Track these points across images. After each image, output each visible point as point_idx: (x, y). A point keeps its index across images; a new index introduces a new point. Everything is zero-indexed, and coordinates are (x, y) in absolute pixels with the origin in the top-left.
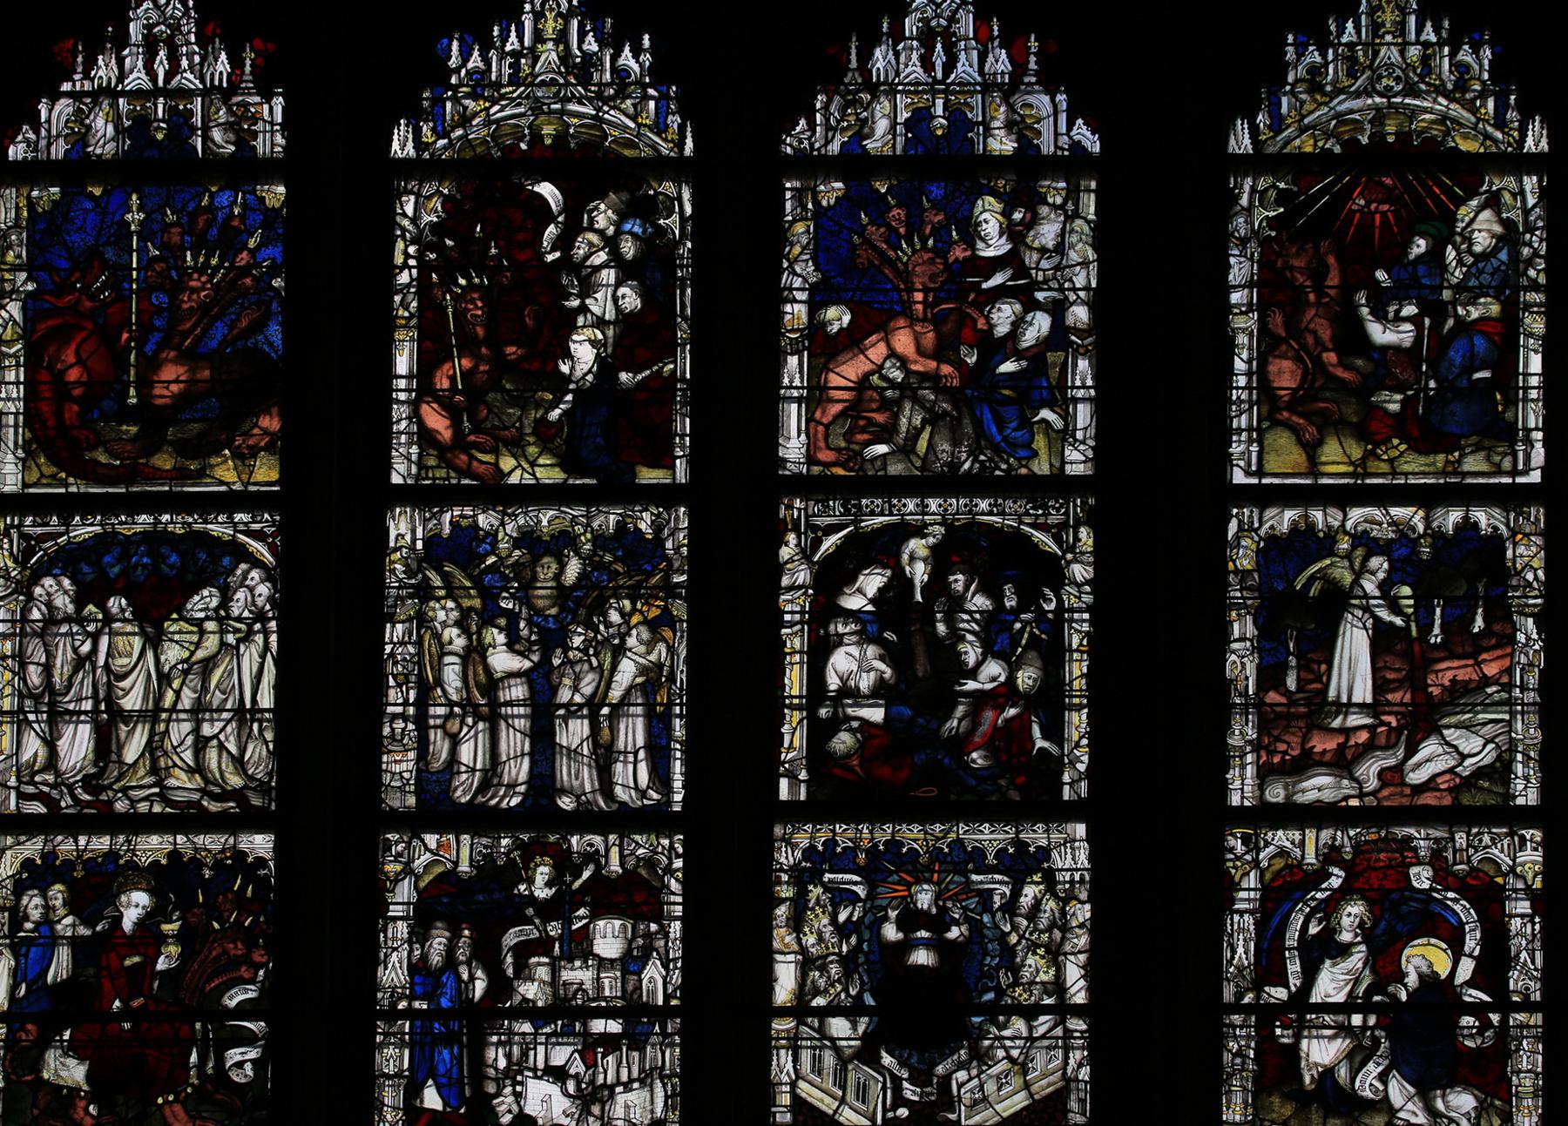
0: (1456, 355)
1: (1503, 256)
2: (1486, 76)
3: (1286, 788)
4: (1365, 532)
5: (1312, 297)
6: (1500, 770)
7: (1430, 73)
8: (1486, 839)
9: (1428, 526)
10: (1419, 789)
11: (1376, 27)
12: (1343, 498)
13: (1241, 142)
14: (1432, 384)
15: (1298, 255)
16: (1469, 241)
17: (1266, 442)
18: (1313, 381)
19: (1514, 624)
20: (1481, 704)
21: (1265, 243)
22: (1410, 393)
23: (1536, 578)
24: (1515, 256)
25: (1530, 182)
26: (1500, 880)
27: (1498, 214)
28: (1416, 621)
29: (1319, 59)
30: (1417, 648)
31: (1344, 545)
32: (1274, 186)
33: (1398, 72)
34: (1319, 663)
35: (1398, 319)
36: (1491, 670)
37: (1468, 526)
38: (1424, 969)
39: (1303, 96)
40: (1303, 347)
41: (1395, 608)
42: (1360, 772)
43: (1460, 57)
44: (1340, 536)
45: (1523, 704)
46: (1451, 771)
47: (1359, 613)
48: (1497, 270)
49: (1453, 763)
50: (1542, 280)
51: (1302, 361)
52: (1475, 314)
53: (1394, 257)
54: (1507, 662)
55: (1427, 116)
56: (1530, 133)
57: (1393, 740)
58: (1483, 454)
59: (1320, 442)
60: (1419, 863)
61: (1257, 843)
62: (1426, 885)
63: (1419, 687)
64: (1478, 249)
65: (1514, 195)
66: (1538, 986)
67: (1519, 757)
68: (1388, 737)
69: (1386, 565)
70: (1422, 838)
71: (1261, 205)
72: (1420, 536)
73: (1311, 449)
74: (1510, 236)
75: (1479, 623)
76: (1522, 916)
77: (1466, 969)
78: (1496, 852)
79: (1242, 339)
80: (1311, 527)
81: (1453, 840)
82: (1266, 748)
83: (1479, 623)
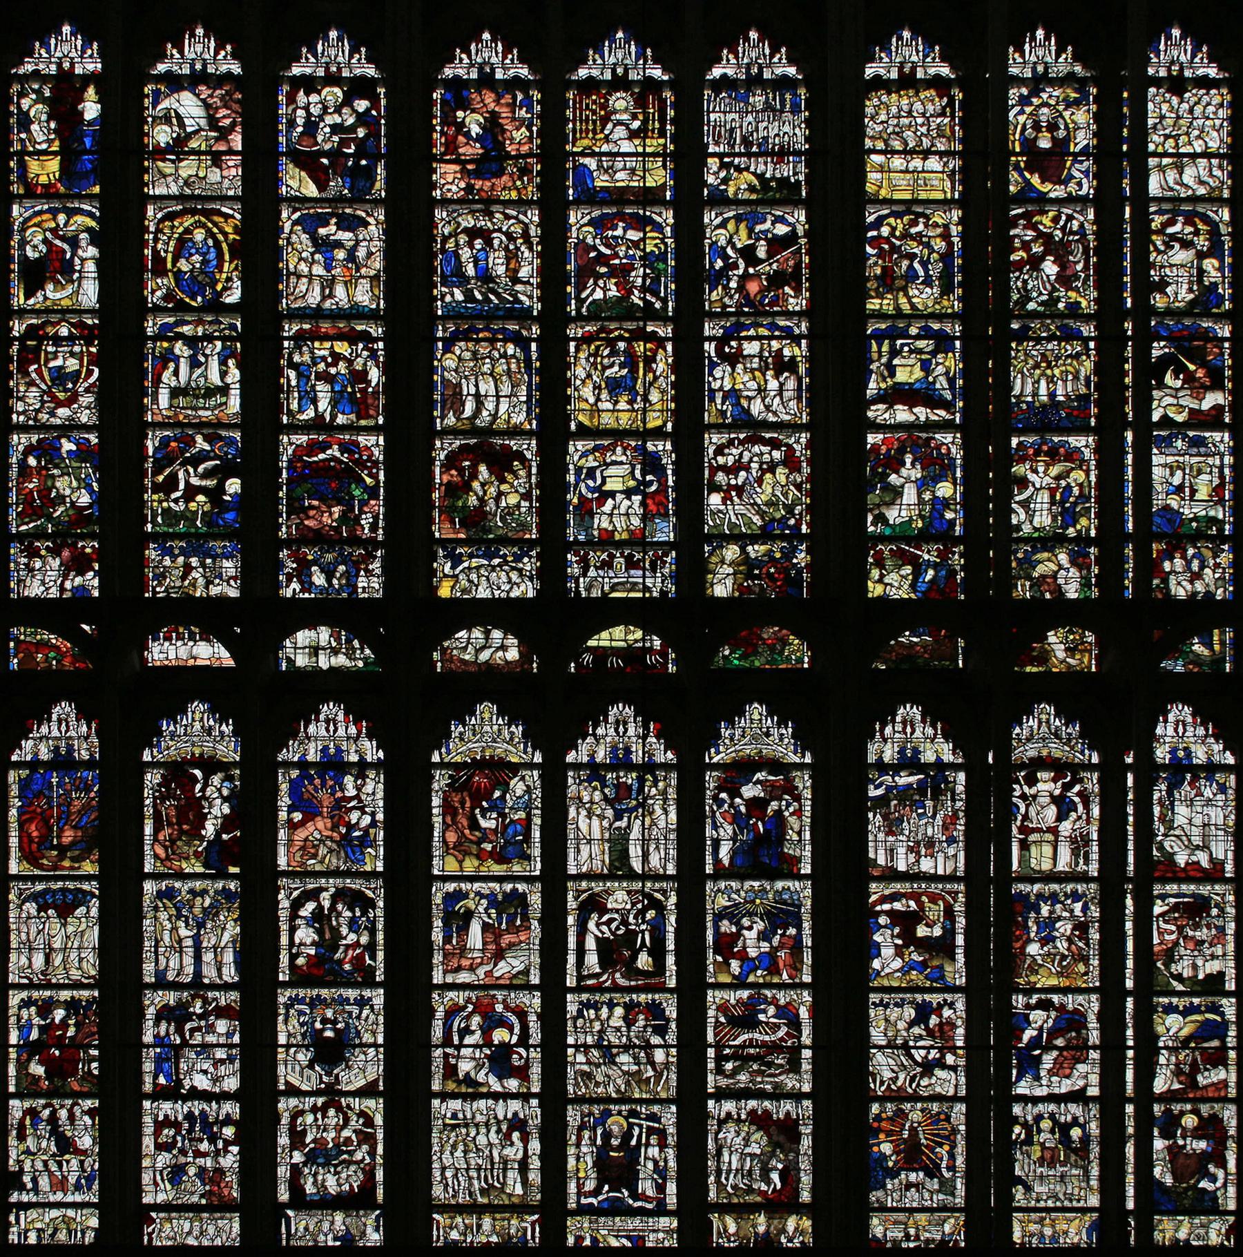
0: (510, 831)
6: (526, 972)
10: (498, 978)
12: (472, 879)
13: (436, 758)
21: (444, 792)
24: (530, 798)
25: (535, 773)
31: (472, 895)
36: (522, 938)
37: (515, 890)
41: (490, 917)
53: (488, 797)
63: (498, 944)
70: (500, 995)
73: (461, 862)
74: (529, 790)
75: (518, 922)
79: (436, 825)
83: (518, 922)
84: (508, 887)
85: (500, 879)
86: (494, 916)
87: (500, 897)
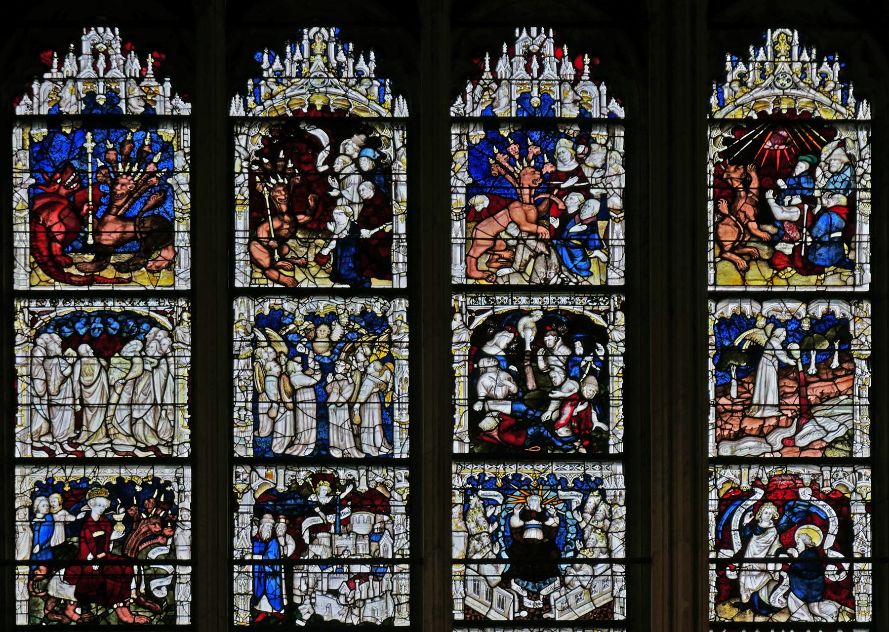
0: (822, 224)
1: (848, 173)
2: (836, 80)
3: (731, 447)
4: (773, 316)
5: (743, 194)
6: (849, 439)
7: (806, 77)
8: (841, 474)
9: (807, 313)
10: (802, 449)
11: (776, 53)
12: (760, 298)
14: (809, 239)
15: (735, 171)
16: (829, 165)
17: (718, 269)
18: (744, 237)
19: (855, 364)
20: (837, 405)
22: (797, 244)
23: (867, 340)
24: (854, 175)
25: (863, 135)
26: (848, 495)
27: (845, 151)
28: (802, 362)
29: (744, 69)
30: (802, 375)
31: (761, 322)
32: (721, 135)
33: (789, 76)
34: (749, 383)
35: (790, 205)
36: (843, 387)
37: (829, 314)
38: (808, 541)
39: (737, 89)
40: (738, 219)
41: (790, 355)
42: (771, 439)
43: (822, 69)
44: (759, 318)
45: (860, 405)
46: (821, 439)
47: (771, 358)
48: (845, 180)
49: (821, 436)
50: (869, 185)
51: (737, 226)
52: (832, 203)
54: (850, 384)
55: (805, 100)
56: (861, 109)
57: (789, 423)
58: (837, 276)
59: (748, 269)
60: (804, 486)
61: (715, 476)
62: (808, 498)
64: (833, 169)
65: (854, 141)
66: (870, 549)
67: (858, 432)
68: (787, 422)
69: (785, 333)
70: (806, 473)
71: (714, 144)
72: (803, 318)
73: (743, 272)
74: (852, 162)
75: (835, 364)
76: (861, 514)
77: (830, 541)
78: (846, 481)
80: (743, 314)
81: (822, 474)
82: (720, 427)
83: (835, 364)
84: (819, 309)
85: (806, 298)
86: (797, 354)
87: (806, 326)
